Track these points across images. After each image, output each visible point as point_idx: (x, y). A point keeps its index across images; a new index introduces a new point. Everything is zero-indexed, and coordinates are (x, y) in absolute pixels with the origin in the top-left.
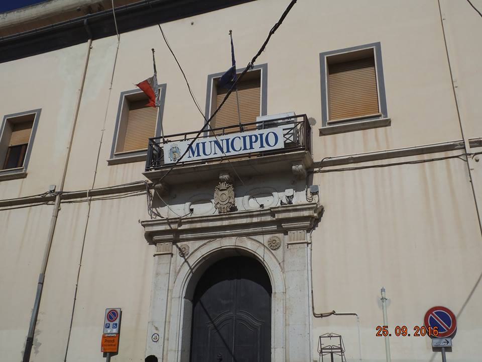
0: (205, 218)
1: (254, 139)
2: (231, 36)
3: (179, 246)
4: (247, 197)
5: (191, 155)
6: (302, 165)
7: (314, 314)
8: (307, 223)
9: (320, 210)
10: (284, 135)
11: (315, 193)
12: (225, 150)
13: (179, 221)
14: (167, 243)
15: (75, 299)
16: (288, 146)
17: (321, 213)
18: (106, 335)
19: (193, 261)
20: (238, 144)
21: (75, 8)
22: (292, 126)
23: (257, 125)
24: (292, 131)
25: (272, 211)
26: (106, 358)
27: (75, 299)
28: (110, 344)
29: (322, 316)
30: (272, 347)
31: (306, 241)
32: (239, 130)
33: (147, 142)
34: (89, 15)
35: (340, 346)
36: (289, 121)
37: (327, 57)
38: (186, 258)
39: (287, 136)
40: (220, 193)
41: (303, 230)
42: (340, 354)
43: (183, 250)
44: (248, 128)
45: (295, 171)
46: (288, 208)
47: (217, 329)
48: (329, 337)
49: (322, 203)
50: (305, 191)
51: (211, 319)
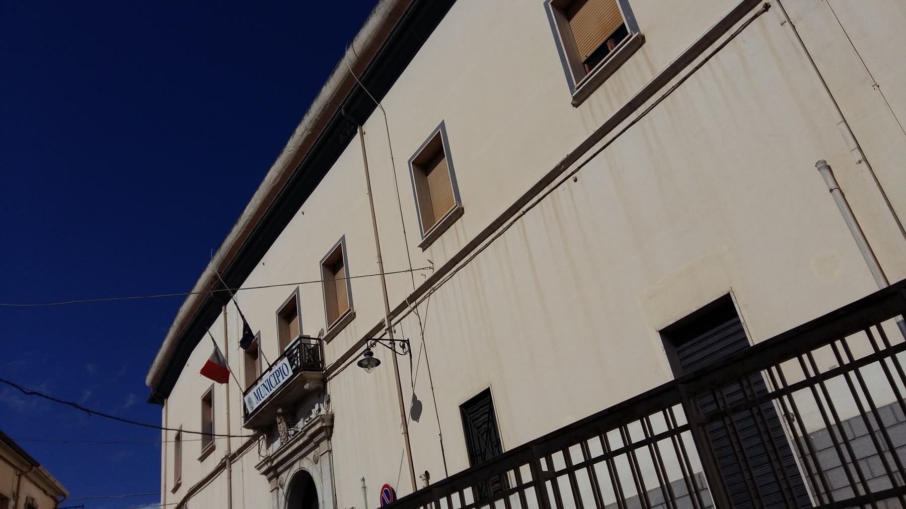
6: (309, 383)
8: (323, 434)
21: (209, 282)
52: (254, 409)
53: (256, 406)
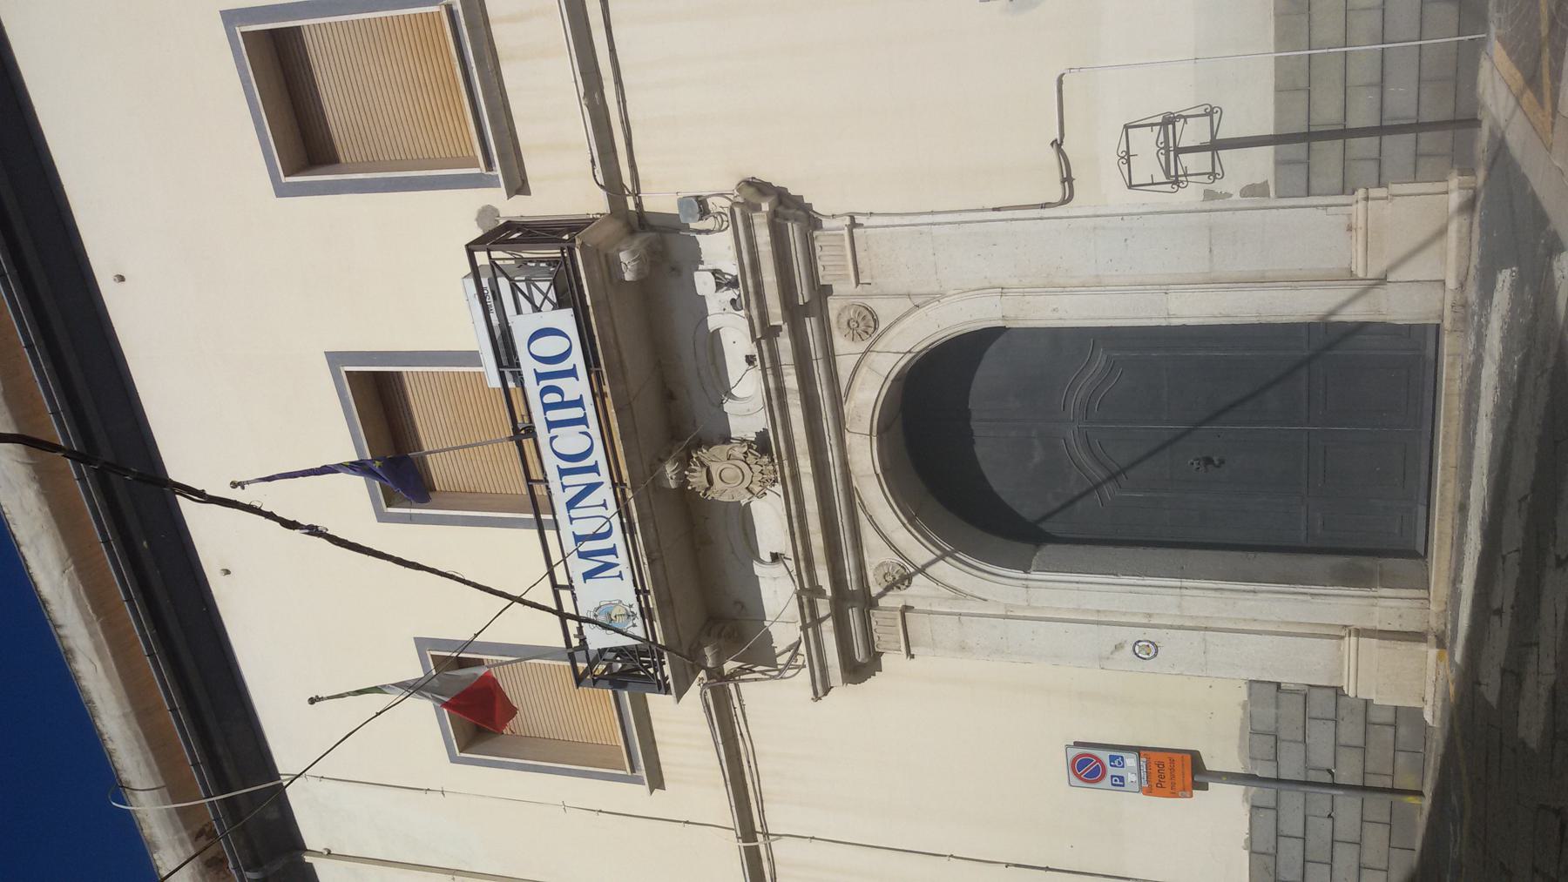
0: (796, 525)
1: (552, 398)
2: (248, 483)
3: (880, 590)
4: (729, 406)
5: (613, 572)
6: (620, 251)
7: (1064, 201)
8: (794, 231)
9: (751, 190)
10: (537, 309)
11: (701, 206)
12: (591, 478)
13: (808, 594)
14: (874, 624)
15: (1047, 869)
16: (567, 296)
17: (759, 188)
18: (1145, 785)
19: (920, 553)
20: (570, 440)
22: (503, 283)
23: (511, 385)
24: (523, 286)
25: (765, 333)
26: (1210, 784)
27: (1047, 869)
28: (1168, 776)
29: (1067, 180)
30: (1164, 323)
31: (846, 232)
32: (531, 440)
33: (587, 691)
34: (231, 865)
35: (1156, 129)
36: (493, 293)
37: (285, 176)
38: (912, 570)
39: (538, 298)
40: (718, 484)
41: (813, 239)
42: (1179, 125)
43: (890, 578)
44: (524, 412)
45: (639, 271)
46: (751, 289)
47: (1119, 473)
48: (1128, 162)
49: (730, 185)
50: (698, 237)
51: (1088, 492)
52: (636, 609)
53: (629, 597)
